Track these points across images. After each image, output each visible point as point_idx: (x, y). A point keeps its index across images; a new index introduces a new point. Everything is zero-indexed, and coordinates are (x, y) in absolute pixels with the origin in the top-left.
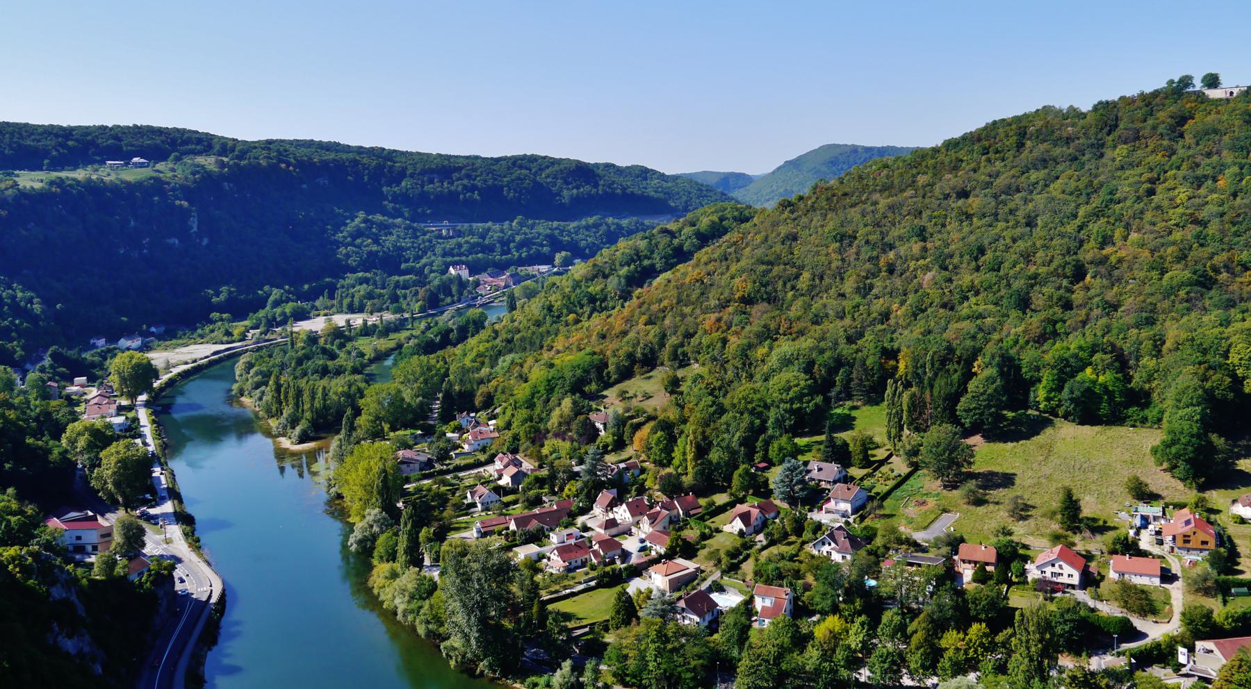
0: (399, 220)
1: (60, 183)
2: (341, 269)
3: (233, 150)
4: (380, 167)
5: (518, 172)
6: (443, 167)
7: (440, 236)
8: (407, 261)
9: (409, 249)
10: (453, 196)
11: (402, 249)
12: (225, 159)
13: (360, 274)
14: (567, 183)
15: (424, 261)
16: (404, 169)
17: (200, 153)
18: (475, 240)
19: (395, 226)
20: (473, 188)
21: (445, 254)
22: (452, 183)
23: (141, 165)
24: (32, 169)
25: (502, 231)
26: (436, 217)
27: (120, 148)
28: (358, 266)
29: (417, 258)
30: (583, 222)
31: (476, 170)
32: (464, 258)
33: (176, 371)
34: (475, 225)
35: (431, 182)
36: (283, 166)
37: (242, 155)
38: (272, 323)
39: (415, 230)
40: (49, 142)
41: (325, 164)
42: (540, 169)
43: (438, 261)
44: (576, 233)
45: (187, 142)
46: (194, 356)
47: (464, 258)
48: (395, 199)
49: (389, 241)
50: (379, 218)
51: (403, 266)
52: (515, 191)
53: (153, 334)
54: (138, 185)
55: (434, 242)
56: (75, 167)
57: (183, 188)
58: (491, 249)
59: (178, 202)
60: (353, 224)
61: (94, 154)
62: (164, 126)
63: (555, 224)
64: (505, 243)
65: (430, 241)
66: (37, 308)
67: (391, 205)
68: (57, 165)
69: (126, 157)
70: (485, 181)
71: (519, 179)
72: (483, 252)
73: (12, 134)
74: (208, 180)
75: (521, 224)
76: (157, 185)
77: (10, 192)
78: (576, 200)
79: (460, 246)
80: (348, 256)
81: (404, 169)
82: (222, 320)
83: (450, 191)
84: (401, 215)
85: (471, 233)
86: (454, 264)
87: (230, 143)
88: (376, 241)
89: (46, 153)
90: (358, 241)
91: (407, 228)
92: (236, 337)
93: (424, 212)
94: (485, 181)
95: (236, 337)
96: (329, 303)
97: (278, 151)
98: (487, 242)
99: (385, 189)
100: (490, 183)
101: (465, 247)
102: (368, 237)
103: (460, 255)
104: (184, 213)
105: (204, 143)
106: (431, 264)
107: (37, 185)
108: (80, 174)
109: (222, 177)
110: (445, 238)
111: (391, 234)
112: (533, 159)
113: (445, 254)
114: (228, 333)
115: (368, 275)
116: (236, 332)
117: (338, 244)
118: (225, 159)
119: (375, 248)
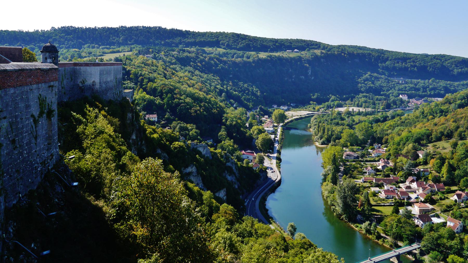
0: (383, 76)
1: (270, 56)
2: (358, 92)
3: (327, 48)
4: (379, 56)
5: (435, 61)
7: (398, 83)
8: (384, 91)
10: (406, 68)
12: (323, 51)
13: (364, 94)
14: (457, 66)
15: (390, 92)
16: (388, 58)
17: (316, 49)
18: (412, 86)
19: (382, 78)
20: (415, 66)
22: (406, 64)
23: (297, 52)
25: (424, 83)
26: (398, 76)
28: (364, 91)
30: (462, 83)
31: (417, 59)
32: (406, 92)
33: (294, 118)
34: (413, 80)
35: (398, 63)
36: (343, 54)
38: (329, 107)
39: (389, 80)
40: (271, 44)
41: (358, 54)
42: (446, 60)
43: (396, 93)
44: (458, 87)
45: (313, 45)
46: (301, 114)
47: (406, 92)
48: (383, 68)
49: (378, 83)
50: (375, 75)
51: (382, 93)
52: (433, 68)
53: (291, 106)
54: (294, 59)
55: (396, 85)
57: (308, 60)
58: (418, 90)
59: (305, 65)
61: (284, 48)
62: (306, 39)
63: (449, 82)
64: (425, 88)
65: (394, 85)
66: (259, 94)
67: (381, 70)
68: (272, 51)
69: (293, 49)
70: (420, 64)
71: (435, 63)
73: (261, 41)
74: (316, 58)
75: (433, 81)
76: (300, 59)
77: (256, 59)
79: (406, 87)
80: (361, 87)
81: (388, 58)
82: (313, 104)
83: (405, 67)
84: (385, 74)
85: (411, 83)
86: (402, 94)
87: (326, 46)
88: (373, 83)
89: (269, 47)
90: (366, 82)
92: (316, 110)
93: (393, 74)
94: (420, 64)
95: (316, 110)
96: (351, 103)
97: (342, 50)
98: (417, 87)
99: (379, 64)
101: (408, 88)
103: (404, 91)
104: (307, 68)
105: (317, 45)
106: (393, 93)
108: (277, 54)
109: (321, 57)
111: (379, 81)
112: (443, 56)
114: (314, 109)
115: (367, 95)
116: (316, 108)
117: (358, 83)
118: (323, 51)
119: (372, 85)
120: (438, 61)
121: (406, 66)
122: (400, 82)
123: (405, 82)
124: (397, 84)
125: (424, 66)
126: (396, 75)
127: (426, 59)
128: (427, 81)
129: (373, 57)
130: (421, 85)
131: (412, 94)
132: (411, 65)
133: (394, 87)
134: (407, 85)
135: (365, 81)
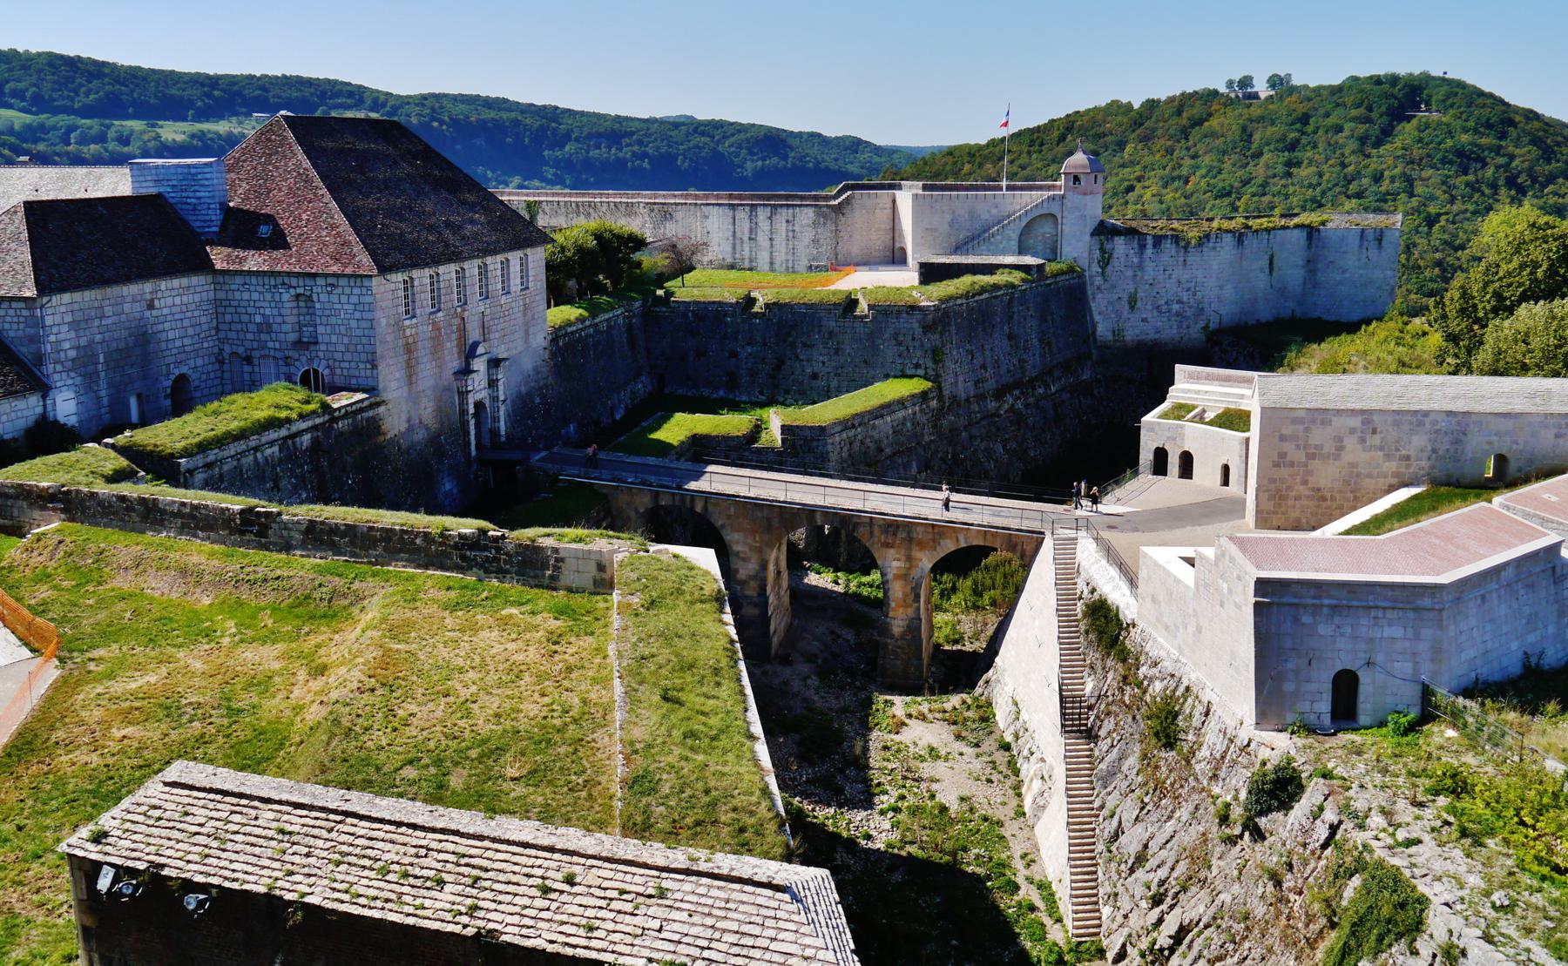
3: (384, 105)
4: (543, 129)
10: (621, 163)
14: (752, 154)
20: (644, 155)
22: (621, 150)
24: (176, 120)
27: (266, 100)
35: (598, 147)
36: (435, 124)
37: (395, 109)
41: (483, 124)
45: (335, 95)
48: (557, 164)
56: (220, 117)
71: (697, 146)
83: (618, 159)
87: (382, 98)
97: (433, 109)
100: (663, 150)
107: (179, 138)
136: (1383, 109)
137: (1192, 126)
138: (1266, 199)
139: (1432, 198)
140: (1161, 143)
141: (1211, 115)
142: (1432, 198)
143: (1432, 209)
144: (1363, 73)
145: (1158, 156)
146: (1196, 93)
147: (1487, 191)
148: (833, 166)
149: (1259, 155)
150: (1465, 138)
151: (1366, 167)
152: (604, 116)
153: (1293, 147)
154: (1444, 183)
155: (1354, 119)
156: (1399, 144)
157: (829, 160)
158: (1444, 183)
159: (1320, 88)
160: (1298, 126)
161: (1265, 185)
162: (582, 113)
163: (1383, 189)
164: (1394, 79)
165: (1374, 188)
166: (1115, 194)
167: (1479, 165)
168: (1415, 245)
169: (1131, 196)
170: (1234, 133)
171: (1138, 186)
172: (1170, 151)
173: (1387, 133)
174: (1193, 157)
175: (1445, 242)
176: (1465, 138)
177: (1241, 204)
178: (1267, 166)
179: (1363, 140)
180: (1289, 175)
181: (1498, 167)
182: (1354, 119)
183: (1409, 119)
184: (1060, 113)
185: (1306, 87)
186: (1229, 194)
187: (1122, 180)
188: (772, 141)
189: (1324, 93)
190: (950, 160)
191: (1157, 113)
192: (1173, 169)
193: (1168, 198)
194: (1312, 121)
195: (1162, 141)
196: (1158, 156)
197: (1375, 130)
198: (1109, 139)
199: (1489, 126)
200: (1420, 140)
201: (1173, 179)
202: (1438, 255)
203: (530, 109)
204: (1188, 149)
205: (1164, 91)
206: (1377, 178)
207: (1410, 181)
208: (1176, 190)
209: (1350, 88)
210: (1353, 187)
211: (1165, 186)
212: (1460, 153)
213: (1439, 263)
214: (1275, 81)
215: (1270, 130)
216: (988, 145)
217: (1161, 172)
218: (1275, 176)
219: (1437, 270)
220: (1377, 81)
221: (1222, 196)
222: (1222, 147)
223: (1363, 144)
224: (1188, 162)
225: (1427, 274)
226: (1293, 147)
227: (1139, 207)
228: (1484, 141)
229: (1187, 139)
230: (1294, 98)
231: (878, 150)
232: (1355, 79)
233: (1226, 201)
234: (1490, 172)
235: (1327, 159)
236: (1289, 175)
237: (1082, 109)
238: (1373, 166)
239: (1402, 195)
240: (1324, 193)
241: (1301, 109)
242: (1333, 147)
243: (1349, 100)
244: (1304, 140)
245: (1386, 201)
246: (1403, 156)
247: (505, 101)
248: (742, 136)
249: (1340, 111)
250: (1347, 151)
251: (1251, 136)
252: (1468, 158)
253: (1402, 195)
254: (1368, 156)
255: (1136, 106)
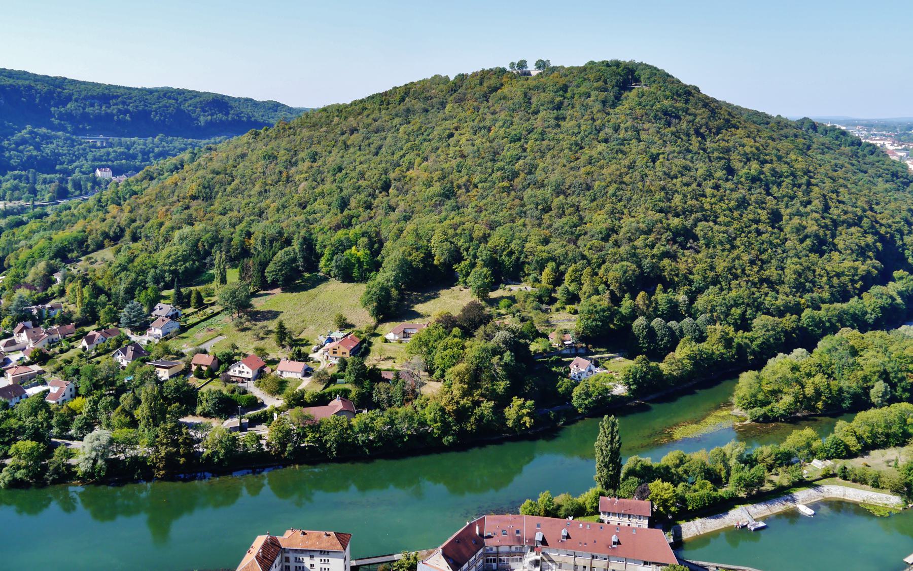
0: (60, 133)
5: (165, 101)
6: (104, 94)
7: (94, 146)
8: (62, 163)
9: (65, 155)
10: (109, 116)
11: (60, 155)
13: (16, 172)
14: (204, 111)
19: (58, 137)
20: (127, 112)
21: (95, 160)
22: (109, 107)
25: (145, 144)
26: (94, 132)
29: (72, 161)
32: (110, 163)
34: (123, 139)
35: (92, 105)
39: (73, 141)
42: (185, 100)
47: (110, 163)
49: (48, 149)
50: (43, 130)
51: (58, 167)
52: (161, 115)
55: (88, 150)
58: (134, 157)
60: (19, 134)
63: (190, 140)
65: (84, 150)
67: (57, 122)
70: (137, 106)
71: (165, 106)
72: (126, 159)
75: (161, 140)
78: (210, 124)
79: (108, 154)
80: (10, 158)
83: (107, 113)
84: (63, 128)
85: (120, 144)
86: (100, 167)
88: (38, 147)
90: (21, 147)
91: (66, 139)
93: (84, 128)
98: (131, 152)
99: (53, 109)
100: (141, 108)
101: (113, 155)
102: (31, 145)
103: (106, 161)
110: (99, 148)
111: (52, 143)
112: (181, 92)
113: (95, 160)
115: (23, 173)
119: (35, 153)
120: (172, 101)
121: (109, 111)
122: (99, 144)
123: (107, 142)
124: (90, 147)
125: (144, 111)
126: (90, 129)
127: (148, 97)
128: (150, 139)
129: (37, 93)
130: (139, 148)
131: (121, 166)
132: (119, 110)
133: (84, 155)
134: (110, 150)
135: (18, 144)
136: (614, 82)
137: (491, 92)
138: (545, 143)
139: (653, 143)
140: (470, 103)
141: (502, 85)
142: (653, 143)
143: (654, 150)
144: (598, 59)
145: (469, 112)
146: (491, 70)
147: (684, 138)
148: (260, 120)
149: (536, 112)
150: (667, 103)
151: (609, 121)
152: (100, 85)
153: (559, 107)
154: (658, 132)
155: (596, 89)
156: (627, 106)
157: (258, 116)
158: (658, 132)
159: (572, 68)
160: (561, 93)
161: (543, 133)
162: (84, 83)
163: (621, 136)
164: (618, 64)
165: (616, 136)
166: (440, 139)
167: (677, 121)
168: (647, 176)
169: (452, 141)
170: (519, 97)
171: (456, 133)
172: (477, 109)
173: (618, 98)
174: (492, 114)
175: (665, 173)
176: (667, 103)
177: (528, 146)
178: (544, 120)
179: (604, 102)
180: (559, 126)
181: (690, 122)
182: (596, 89)
183: (631, 89)
184: (401, 83)
185: (563, 67)
186: (519, 139)
187: (445, 129)
188: (219, 103)
189: (575, 72)
190: (325, 114)
191: (466, 83)
192: (480, 121)
193: (478, 142)
194: (569, 89)
195: (471, 102)
196: (469, 112)
197: (611, 96)
198: (434, 100)
199: (679, 96)
200: (640, 104)
201: (480, 128)
202: (662, 183)
203: (45, 79)
204: (489, 108)
205: (469, 69)
206: (617, 129)
207: (637, 131)
208: (483, 136)
209: (592, 68)
210: (602, 135)
211: (475, 134)
212: (666, 113)
213: (663, 189)
214: (540, 64)
215: (543, 95)
216: (351, 104)
217: (471, 123)
218: (549, 127)
219: (663, 193)
220: (608, 65)
221: (515, 141)
222: (512, 107)
223: (604, 106)
224: (489, 117)
225: (657, 196)
226: (559, 107)
227: (457, 148)
228: (678, 105)
229: (487, 101)
230: (556, 74)
231: (290, 110)
232: (592, 63)
233: (518, 144)
234: (684, 125)
235: (583, 116)
236: (559, 126)
237: (415, 81)
238: (613, 121)
239: (634, 141)
240: (583, 139)
241: (563, 81)
242: (585, 107)
243: (592, 77)
244: (566, 104)
245: (623, 144)
246: (631, 114)
247: (25, 73)
248: (197, 99)
249: (587, 83)
250: (595, 110)
251: (530, 99)
252: (670, 116)
253: (634, 141)
254: (608, 114)
255: (452, 78)
